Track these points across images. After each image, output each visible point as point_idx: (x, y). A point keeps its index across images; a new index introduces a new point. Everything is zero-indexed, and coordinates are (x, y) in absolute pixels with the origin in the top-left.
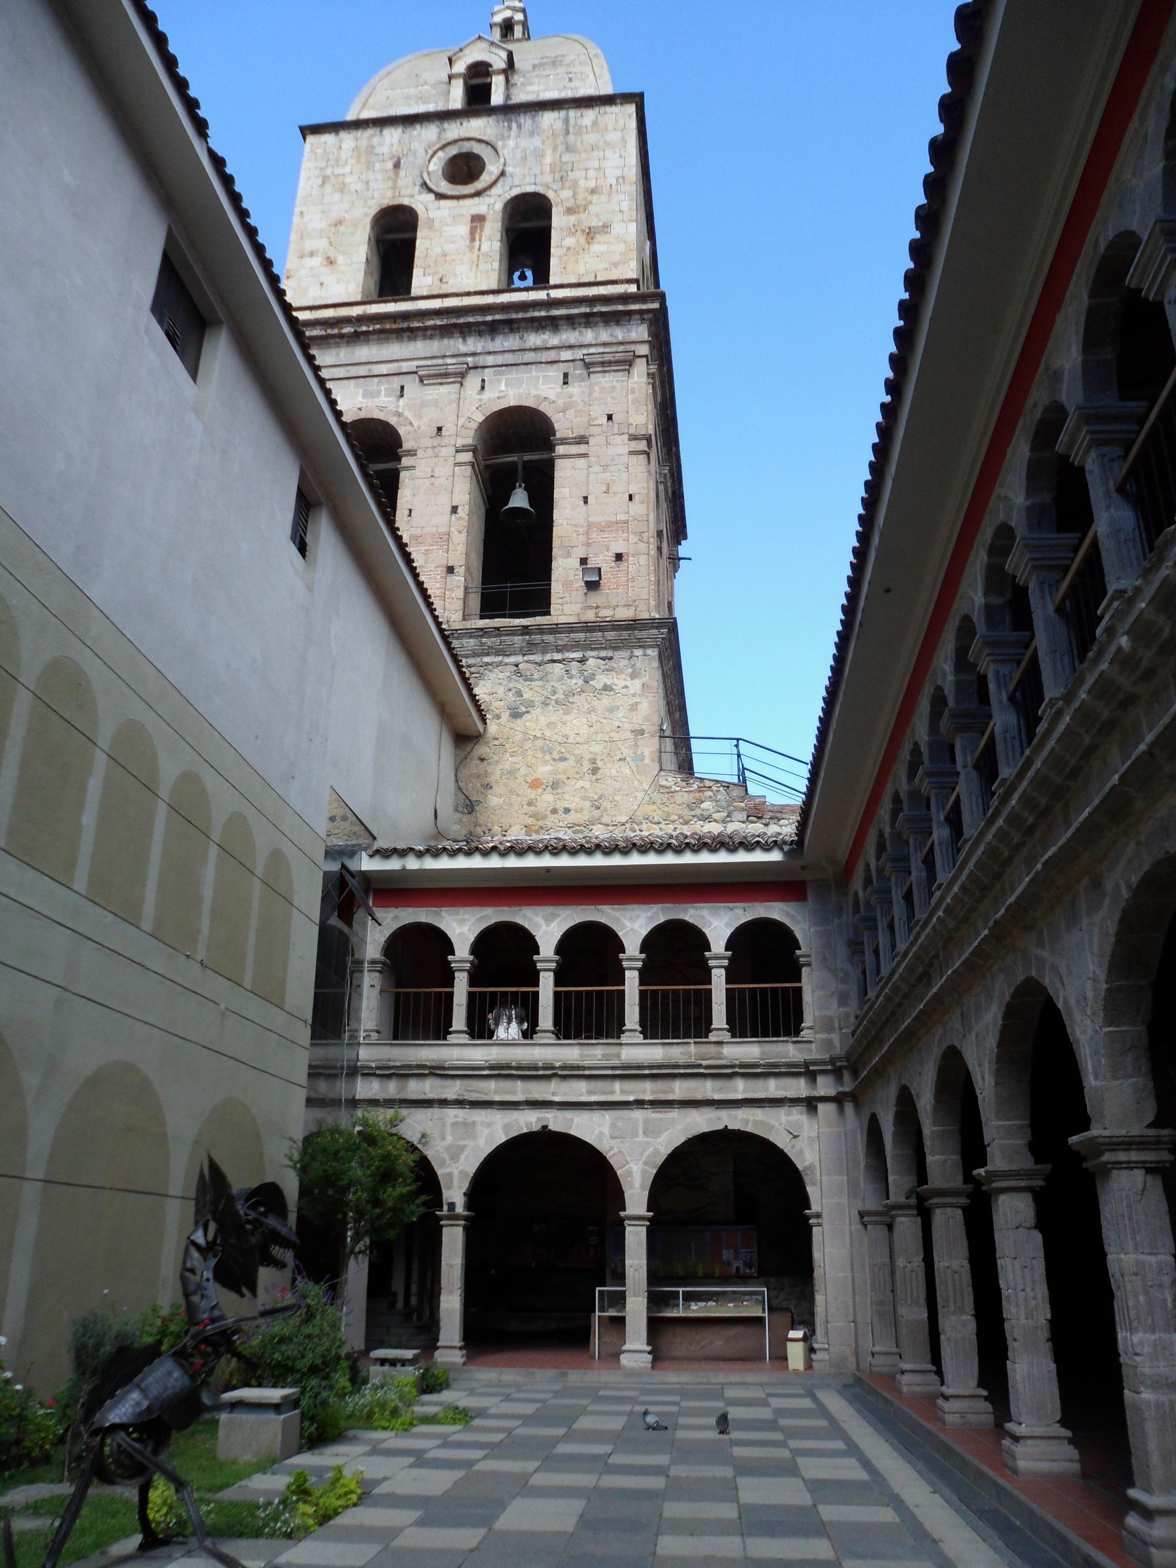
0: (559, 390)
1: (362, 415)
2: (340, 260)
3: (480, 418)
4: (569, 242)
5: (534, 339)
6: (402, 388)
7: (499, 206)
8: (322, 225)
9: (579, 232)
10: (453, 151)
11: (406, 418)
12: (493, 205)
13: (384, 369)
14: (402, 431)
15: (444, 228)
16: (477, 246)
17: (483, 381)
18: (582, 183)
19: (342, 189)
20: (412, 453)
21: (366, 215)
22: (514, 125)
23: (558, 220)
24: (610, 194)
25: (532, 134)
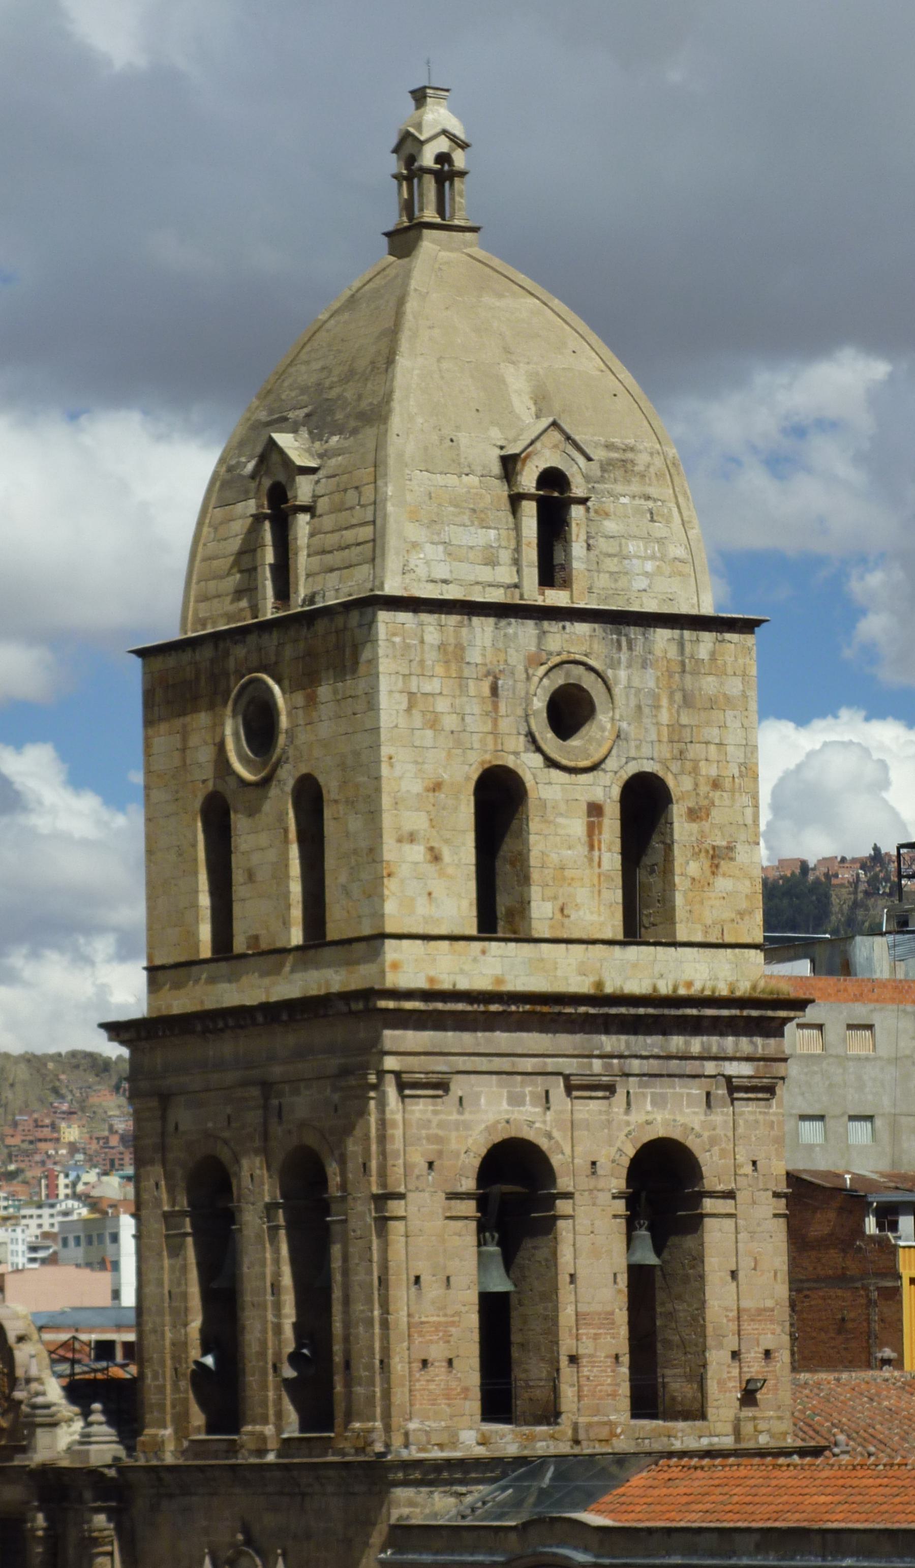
0: (703, 1118)
1: (513, 1133)
3: (631, 1152)
4: (694, 868)
6: (547, 1092)
7: (616, 792)
8: (417, 787)
9: (703, 854)
10: (559, 679)
11: (557, 1142)
13: (528, 1064)
14: (556, 1160)
15: (560, 820)
16: (596, 859)
17: (628, 1093)
18: (704, 768)
19: (433, 722)
21: (468, 778)
22: (623, 639)
24: (733, 791)
25: (644, 666)
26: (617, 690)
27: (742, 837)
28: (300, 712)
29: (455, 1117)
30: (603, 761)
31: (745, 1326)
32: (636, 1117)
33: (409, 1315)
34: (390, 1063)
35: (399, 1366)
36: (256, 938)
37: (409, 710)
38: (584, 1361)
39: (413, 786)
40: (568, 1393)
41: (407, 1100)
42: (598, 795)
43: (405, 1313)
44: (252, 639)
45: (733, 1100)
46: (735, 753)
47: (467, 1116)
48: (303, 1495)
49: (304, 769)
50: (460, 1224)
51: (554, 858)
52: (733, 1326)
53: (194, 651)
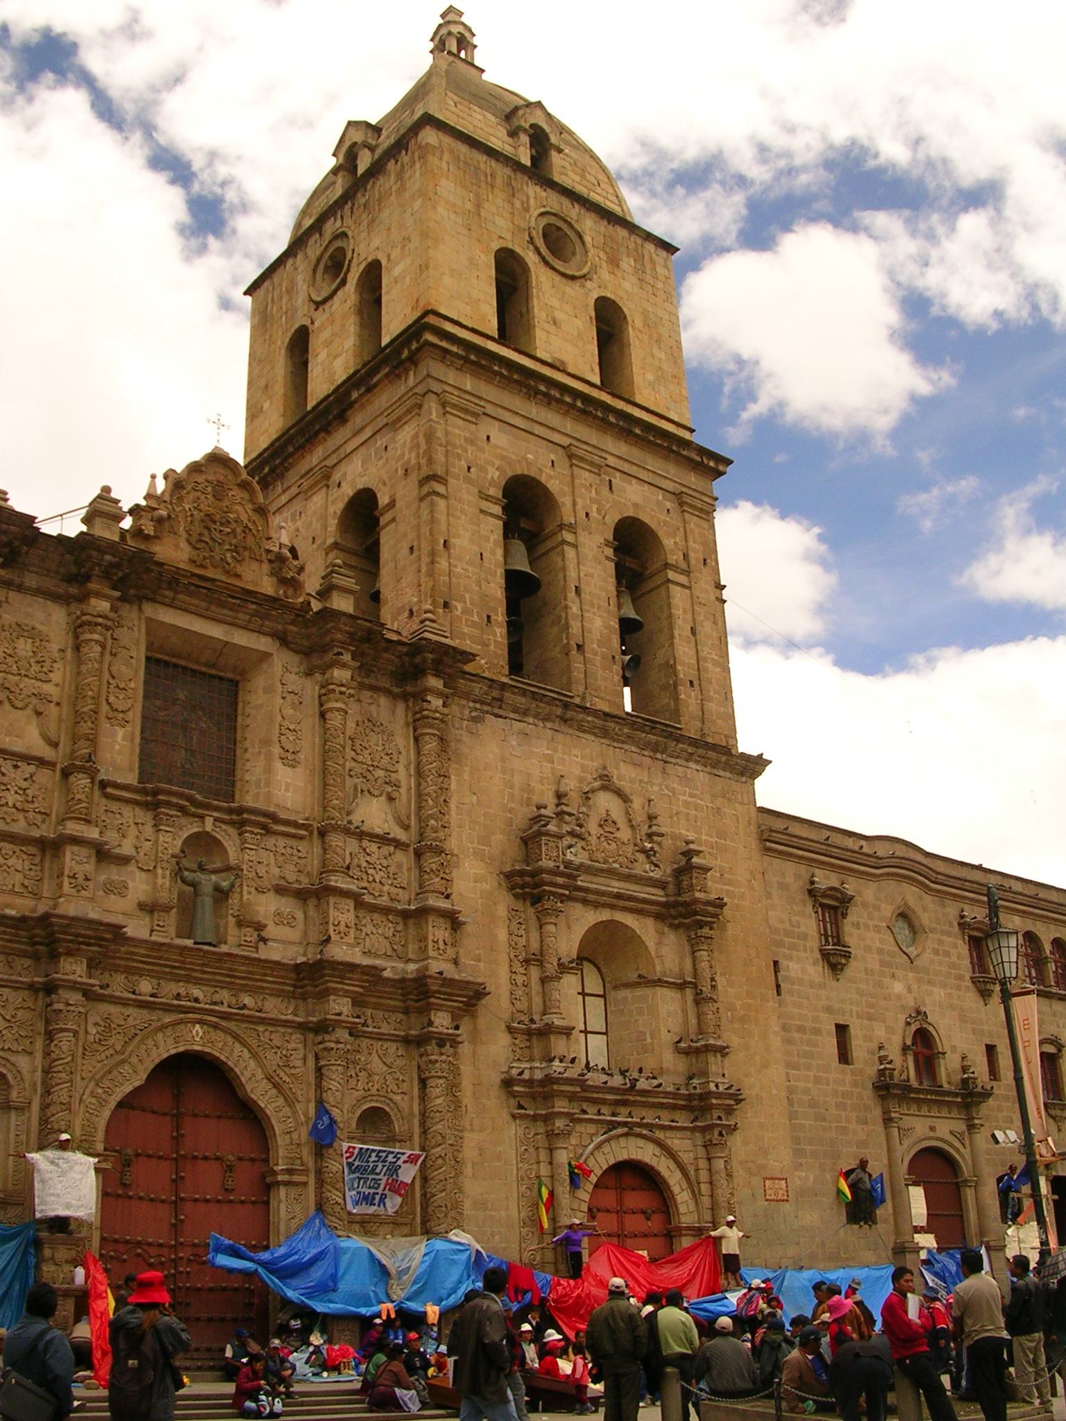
28: (604, 264)
36: (563, 363)
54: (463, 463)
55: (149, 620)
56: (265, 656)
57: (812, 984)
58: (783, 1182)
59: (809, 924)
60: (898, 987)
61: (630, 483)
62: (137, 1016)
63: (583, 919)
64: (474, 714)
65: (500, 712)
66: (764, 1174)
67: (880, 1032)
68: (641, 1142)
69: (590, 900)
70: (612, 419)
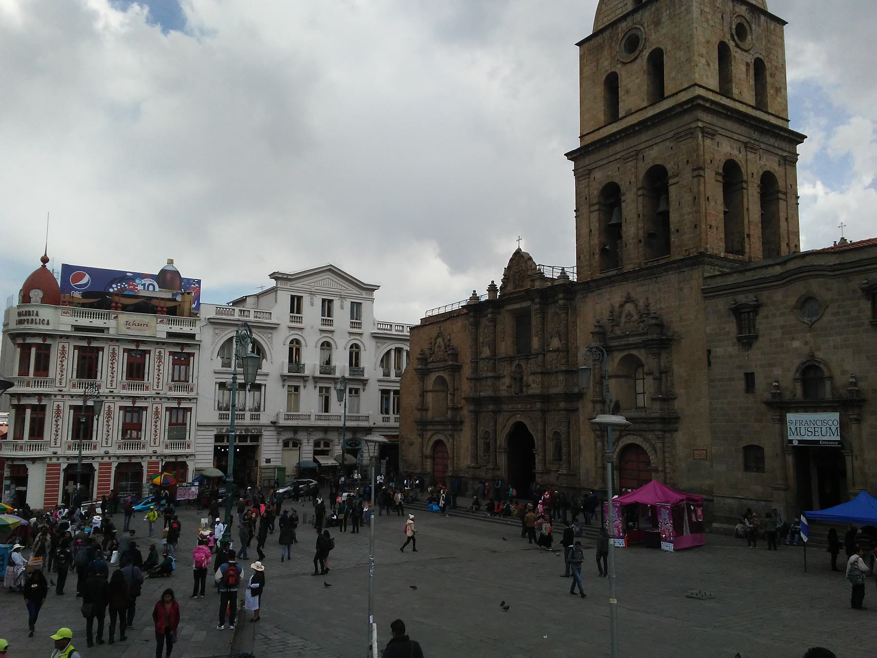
2: (711, 64)
5: (772, 141)
7: (753, 61)
8: (703, 40)
12: (750, 59)
13: (736, 137)
14: (743, 170)
15: (739, 64)
19: (707, 21)
20: (746, 182)
23: (769, 79)
26: (753, 32)
27: (783, 86)
29: (717, 148)
30: (750, 49)
31: (790, 236)
32: (762, 163)
33: (706, 209)
34: (700, 124)
35: (703, 226)
36: (630, 109)
37: (701, 14)
38: (751, 237)
39: (702, 39)
40: (747, 246)
41: (705, 138)
42: (749, 61)
43: (704, 208)
44: (629, 19)
45: (785, 164)
46: (780, 61)
47: (719, 149)
48: (657, 278)
49: (654, 47)
50: (719, 183)
51: (738, 75)
52: (785, 236)
53: (602, 34)
54: (584, 198)
55: (506, 310)
56: (530, 306)
57: (731, 357)
58: (704, 451)
59: (731, 327)
60: (796, 344)
61: (653, 149)
62: (507, 413)
63: (618, 356)
64: (584, 295)
65: (593, 290)
66: (694, 448)
67: (777, 372)
68: (635, 437)
69: (620, 349)
70: (637, 128)
